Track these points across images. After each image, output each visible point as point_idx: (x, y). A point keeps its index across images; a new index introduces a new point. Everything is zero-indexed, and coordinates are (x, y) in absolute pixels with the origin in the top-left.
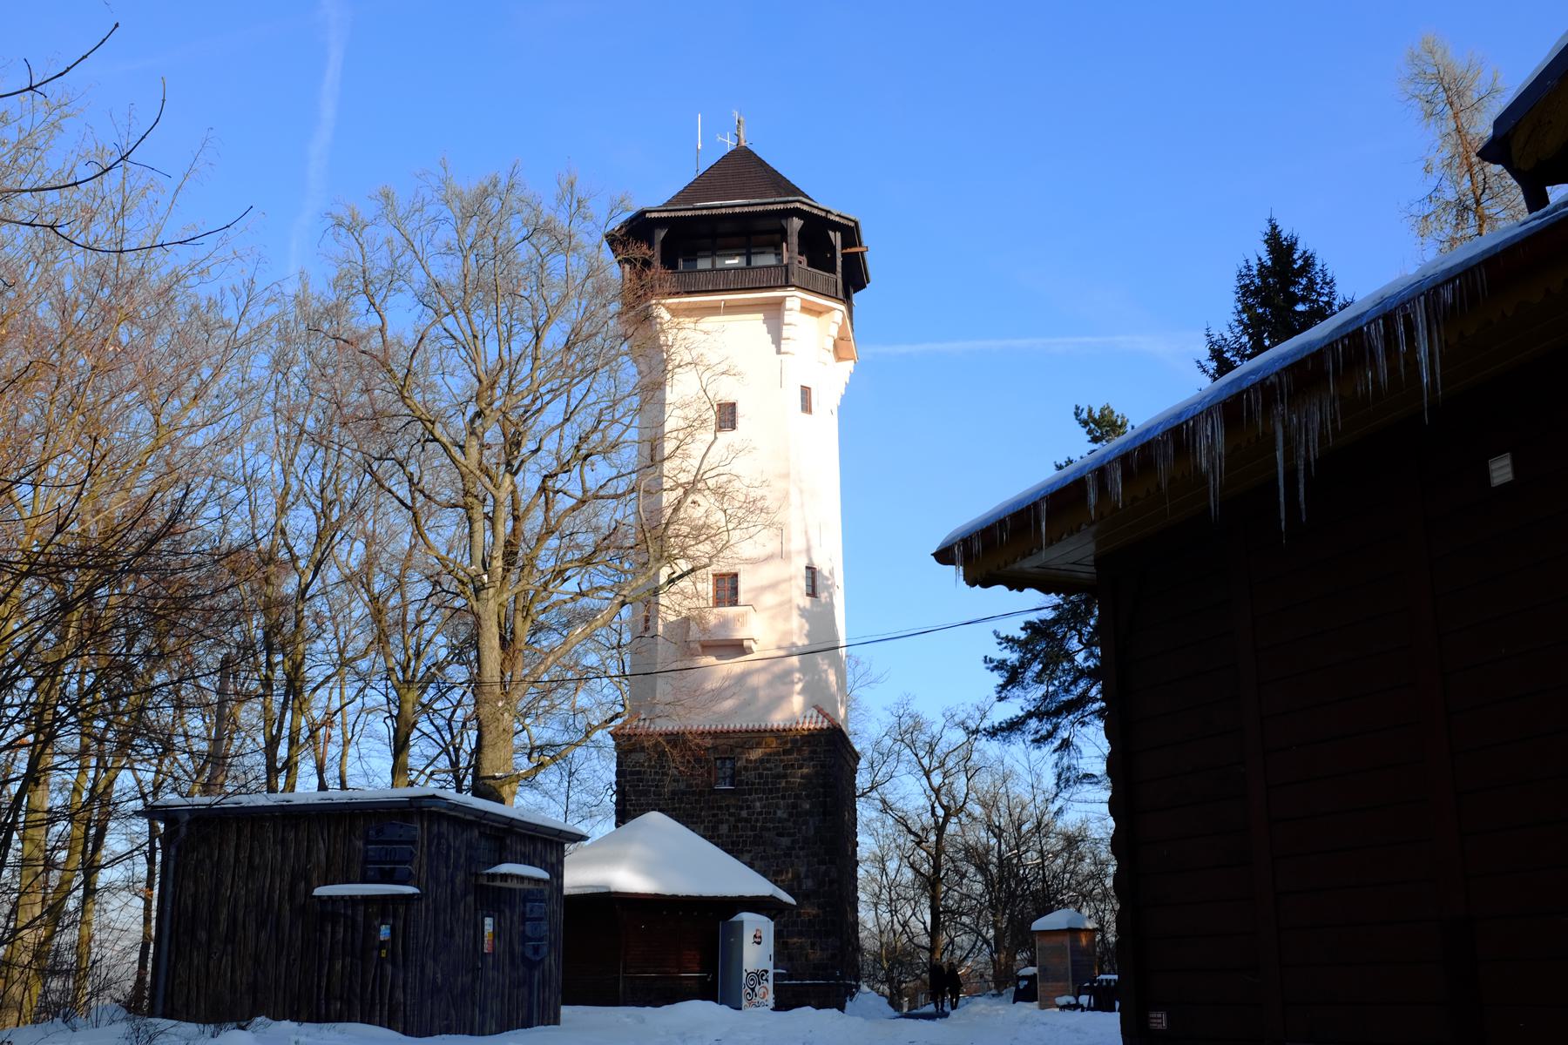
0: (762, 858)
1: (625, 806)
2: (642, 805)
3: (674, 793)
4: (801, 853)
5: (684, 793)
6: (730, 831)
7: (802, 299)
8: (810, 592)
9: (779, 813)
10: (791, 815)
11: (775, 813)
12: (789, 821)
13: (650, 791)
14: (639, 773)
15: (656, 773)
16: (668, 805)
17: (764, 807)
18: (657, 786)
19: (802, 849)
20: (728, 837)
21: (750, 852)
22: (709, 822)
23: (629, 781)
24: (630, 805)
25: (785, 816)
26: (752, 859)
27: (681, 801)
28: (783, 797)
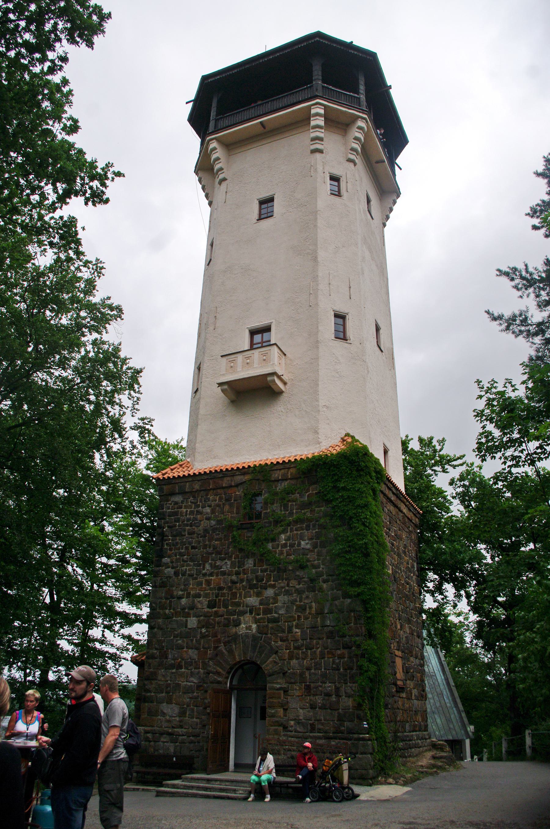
0: (287, 593)
1: (163, 545)
2: (177, 543)
3: (206, 531)
4: (325, 586)
5: (214, 530)
6: (254, 566)
7: (326, 107)
8: (341, 336)
9: (303, 543)
10: (315, 546)
11: (299, 544)
12: (312, 551)
13: (185, 531)
14: (176, 514)
15: (192, 513)
16: (199, 542)
17: (288, 539)
18: (191, 526)
19: (325, 581)
20: (253, 571)
21: (273, 586)
22: (236, 557)
23: (167, 523)
24: (167, 544)
25: (308, 546)
26: (275, 593)
27: (210, 540)
28: (308, 528)
